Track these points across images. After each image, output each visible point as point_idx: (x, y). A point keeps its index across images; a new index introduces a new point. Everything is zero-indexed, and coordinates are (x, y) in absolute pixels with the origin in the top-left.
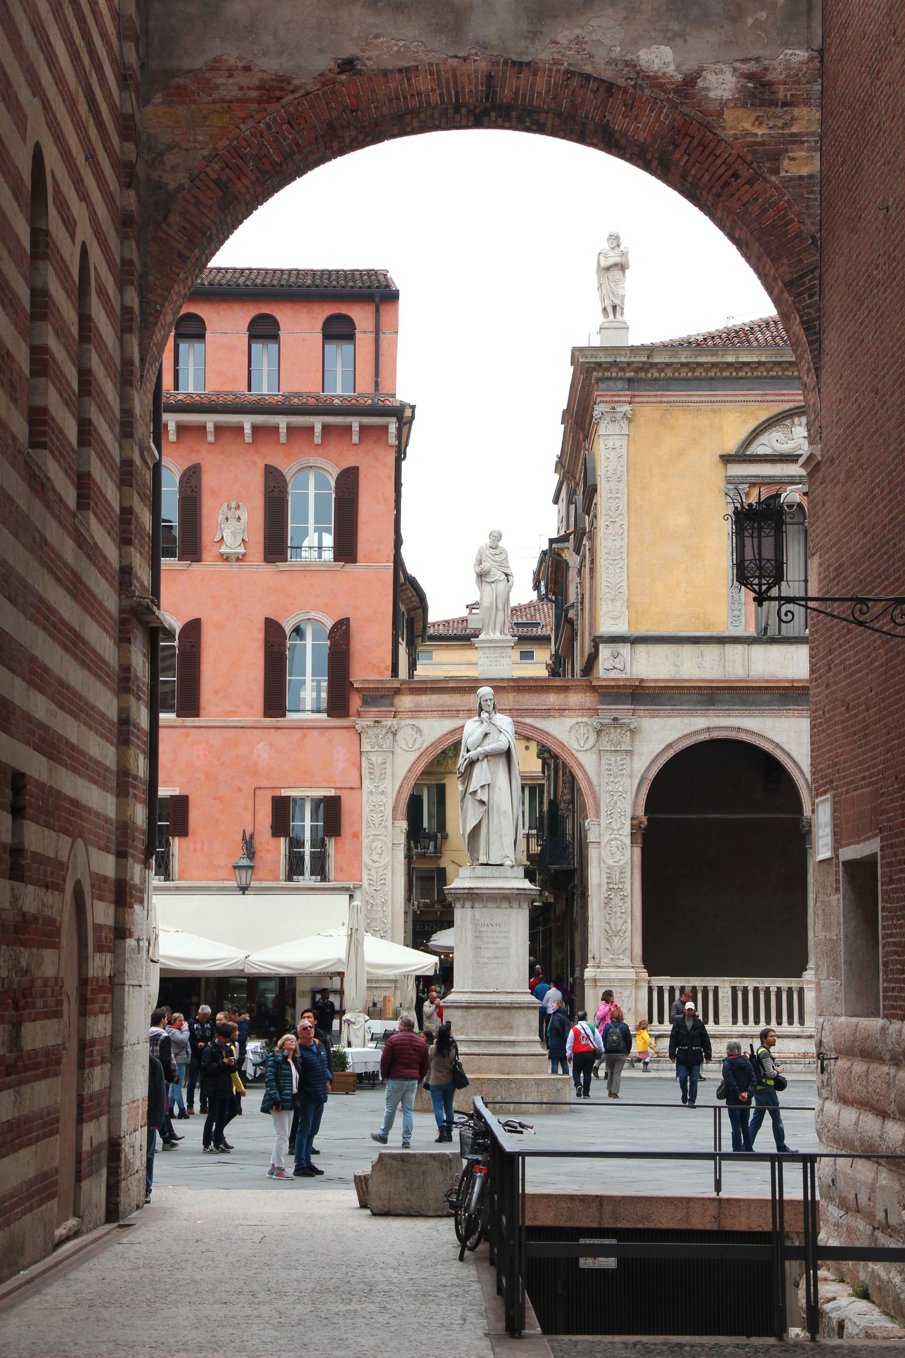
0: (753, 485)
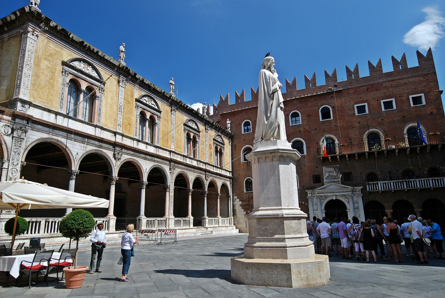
0: (70, 73)
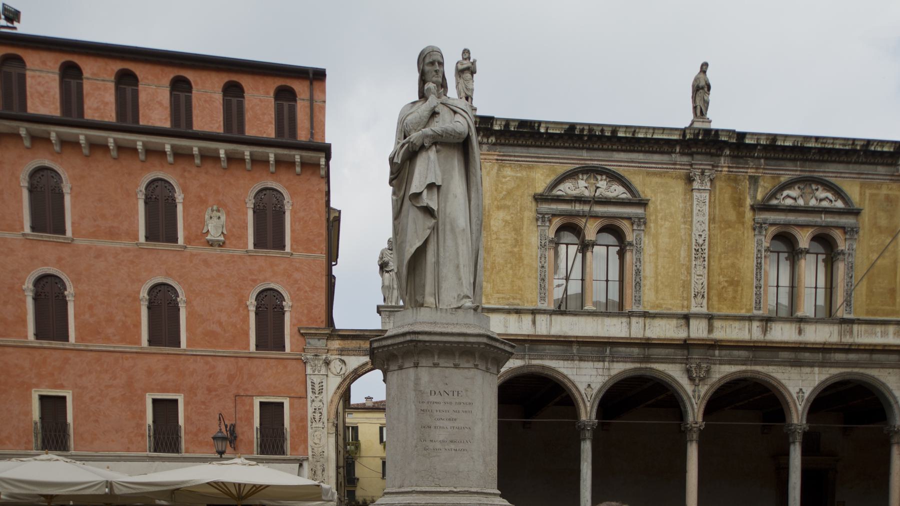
0: (554, 215)
